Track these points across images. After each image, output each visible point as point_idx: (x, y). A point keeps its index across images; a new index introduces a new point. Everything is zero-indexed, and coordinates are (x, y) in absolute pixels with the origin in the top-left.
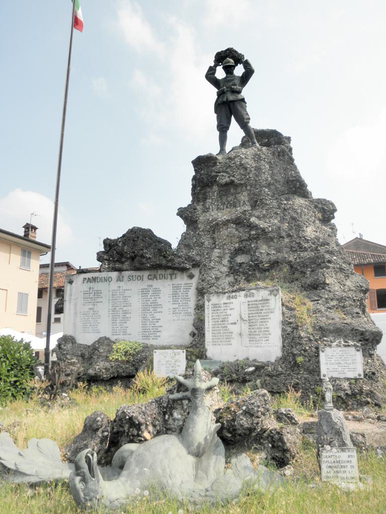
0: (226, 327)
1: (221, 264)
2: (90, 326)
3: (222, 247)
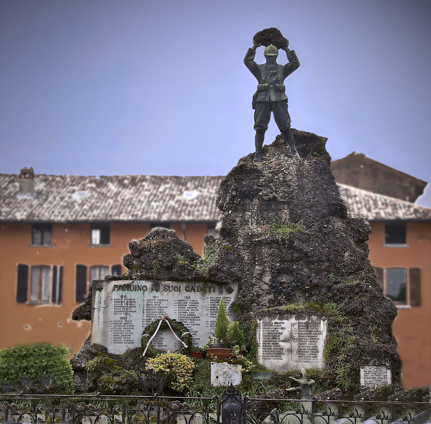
0: (278, 344)
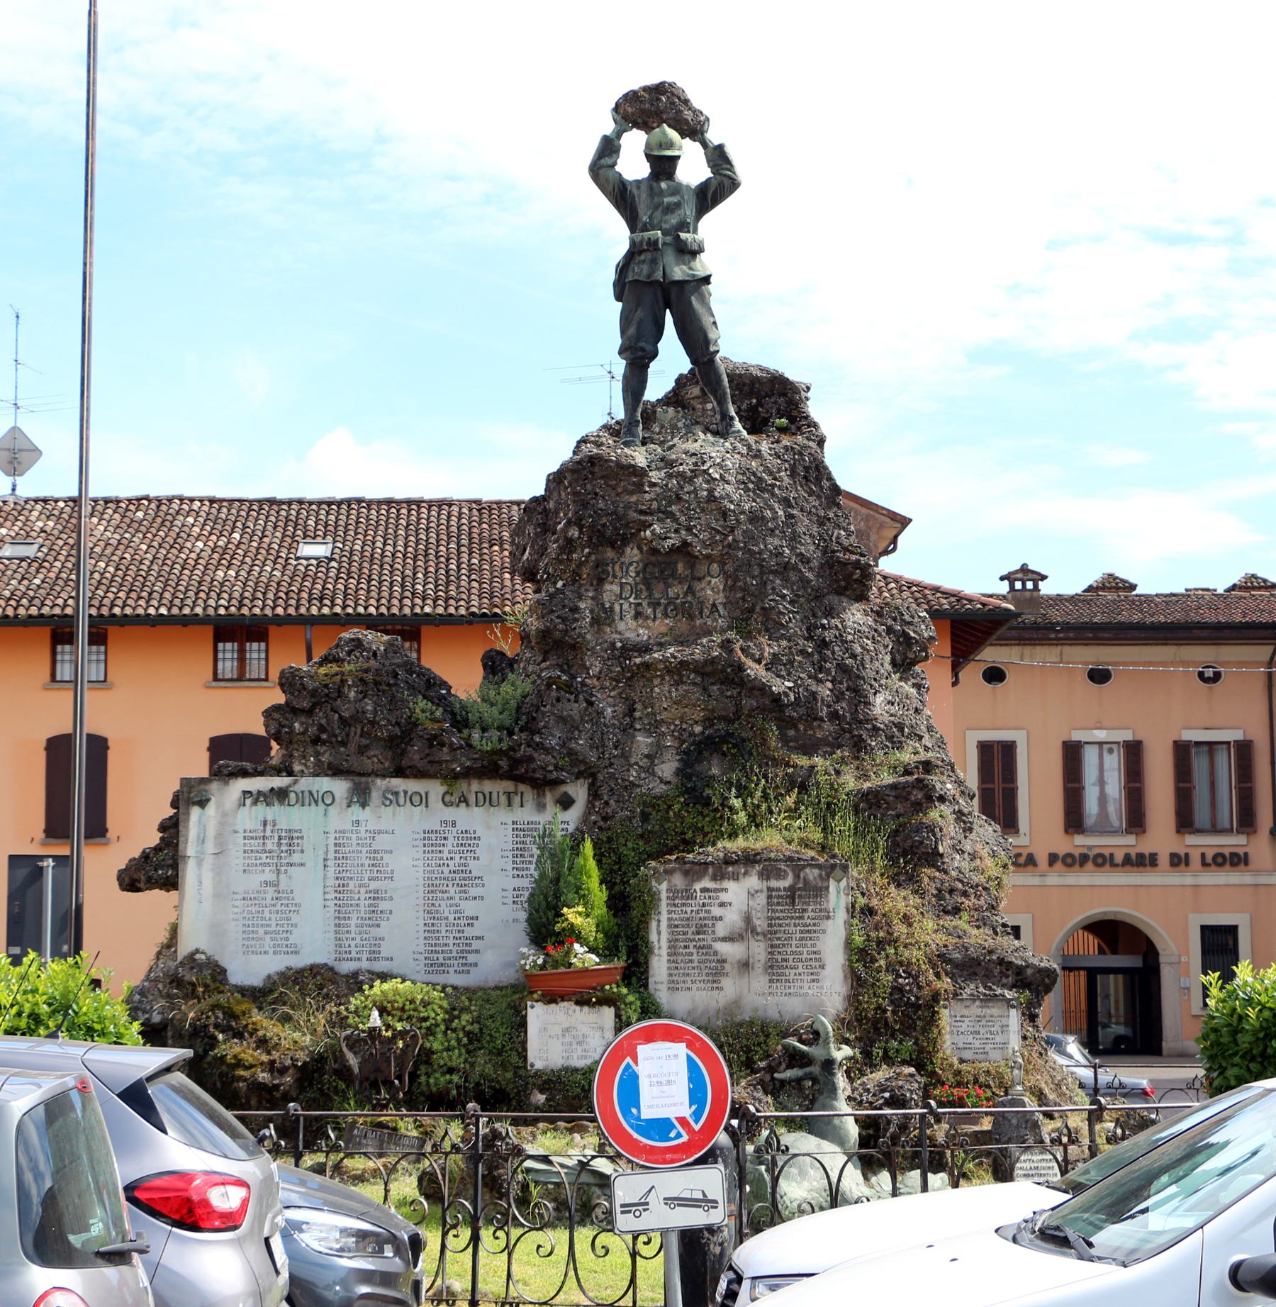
0: (710, 947)
1: (654, 774)
2: (266, 933)
3: (653, 727)
